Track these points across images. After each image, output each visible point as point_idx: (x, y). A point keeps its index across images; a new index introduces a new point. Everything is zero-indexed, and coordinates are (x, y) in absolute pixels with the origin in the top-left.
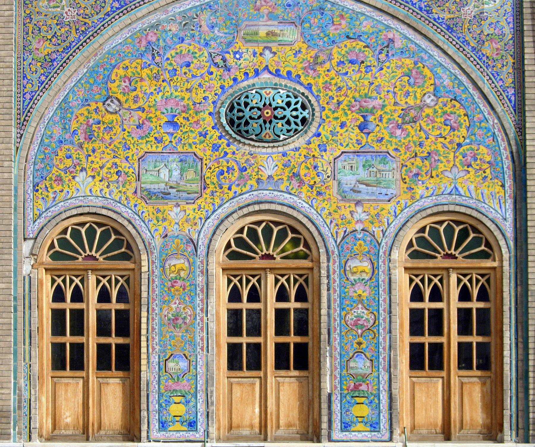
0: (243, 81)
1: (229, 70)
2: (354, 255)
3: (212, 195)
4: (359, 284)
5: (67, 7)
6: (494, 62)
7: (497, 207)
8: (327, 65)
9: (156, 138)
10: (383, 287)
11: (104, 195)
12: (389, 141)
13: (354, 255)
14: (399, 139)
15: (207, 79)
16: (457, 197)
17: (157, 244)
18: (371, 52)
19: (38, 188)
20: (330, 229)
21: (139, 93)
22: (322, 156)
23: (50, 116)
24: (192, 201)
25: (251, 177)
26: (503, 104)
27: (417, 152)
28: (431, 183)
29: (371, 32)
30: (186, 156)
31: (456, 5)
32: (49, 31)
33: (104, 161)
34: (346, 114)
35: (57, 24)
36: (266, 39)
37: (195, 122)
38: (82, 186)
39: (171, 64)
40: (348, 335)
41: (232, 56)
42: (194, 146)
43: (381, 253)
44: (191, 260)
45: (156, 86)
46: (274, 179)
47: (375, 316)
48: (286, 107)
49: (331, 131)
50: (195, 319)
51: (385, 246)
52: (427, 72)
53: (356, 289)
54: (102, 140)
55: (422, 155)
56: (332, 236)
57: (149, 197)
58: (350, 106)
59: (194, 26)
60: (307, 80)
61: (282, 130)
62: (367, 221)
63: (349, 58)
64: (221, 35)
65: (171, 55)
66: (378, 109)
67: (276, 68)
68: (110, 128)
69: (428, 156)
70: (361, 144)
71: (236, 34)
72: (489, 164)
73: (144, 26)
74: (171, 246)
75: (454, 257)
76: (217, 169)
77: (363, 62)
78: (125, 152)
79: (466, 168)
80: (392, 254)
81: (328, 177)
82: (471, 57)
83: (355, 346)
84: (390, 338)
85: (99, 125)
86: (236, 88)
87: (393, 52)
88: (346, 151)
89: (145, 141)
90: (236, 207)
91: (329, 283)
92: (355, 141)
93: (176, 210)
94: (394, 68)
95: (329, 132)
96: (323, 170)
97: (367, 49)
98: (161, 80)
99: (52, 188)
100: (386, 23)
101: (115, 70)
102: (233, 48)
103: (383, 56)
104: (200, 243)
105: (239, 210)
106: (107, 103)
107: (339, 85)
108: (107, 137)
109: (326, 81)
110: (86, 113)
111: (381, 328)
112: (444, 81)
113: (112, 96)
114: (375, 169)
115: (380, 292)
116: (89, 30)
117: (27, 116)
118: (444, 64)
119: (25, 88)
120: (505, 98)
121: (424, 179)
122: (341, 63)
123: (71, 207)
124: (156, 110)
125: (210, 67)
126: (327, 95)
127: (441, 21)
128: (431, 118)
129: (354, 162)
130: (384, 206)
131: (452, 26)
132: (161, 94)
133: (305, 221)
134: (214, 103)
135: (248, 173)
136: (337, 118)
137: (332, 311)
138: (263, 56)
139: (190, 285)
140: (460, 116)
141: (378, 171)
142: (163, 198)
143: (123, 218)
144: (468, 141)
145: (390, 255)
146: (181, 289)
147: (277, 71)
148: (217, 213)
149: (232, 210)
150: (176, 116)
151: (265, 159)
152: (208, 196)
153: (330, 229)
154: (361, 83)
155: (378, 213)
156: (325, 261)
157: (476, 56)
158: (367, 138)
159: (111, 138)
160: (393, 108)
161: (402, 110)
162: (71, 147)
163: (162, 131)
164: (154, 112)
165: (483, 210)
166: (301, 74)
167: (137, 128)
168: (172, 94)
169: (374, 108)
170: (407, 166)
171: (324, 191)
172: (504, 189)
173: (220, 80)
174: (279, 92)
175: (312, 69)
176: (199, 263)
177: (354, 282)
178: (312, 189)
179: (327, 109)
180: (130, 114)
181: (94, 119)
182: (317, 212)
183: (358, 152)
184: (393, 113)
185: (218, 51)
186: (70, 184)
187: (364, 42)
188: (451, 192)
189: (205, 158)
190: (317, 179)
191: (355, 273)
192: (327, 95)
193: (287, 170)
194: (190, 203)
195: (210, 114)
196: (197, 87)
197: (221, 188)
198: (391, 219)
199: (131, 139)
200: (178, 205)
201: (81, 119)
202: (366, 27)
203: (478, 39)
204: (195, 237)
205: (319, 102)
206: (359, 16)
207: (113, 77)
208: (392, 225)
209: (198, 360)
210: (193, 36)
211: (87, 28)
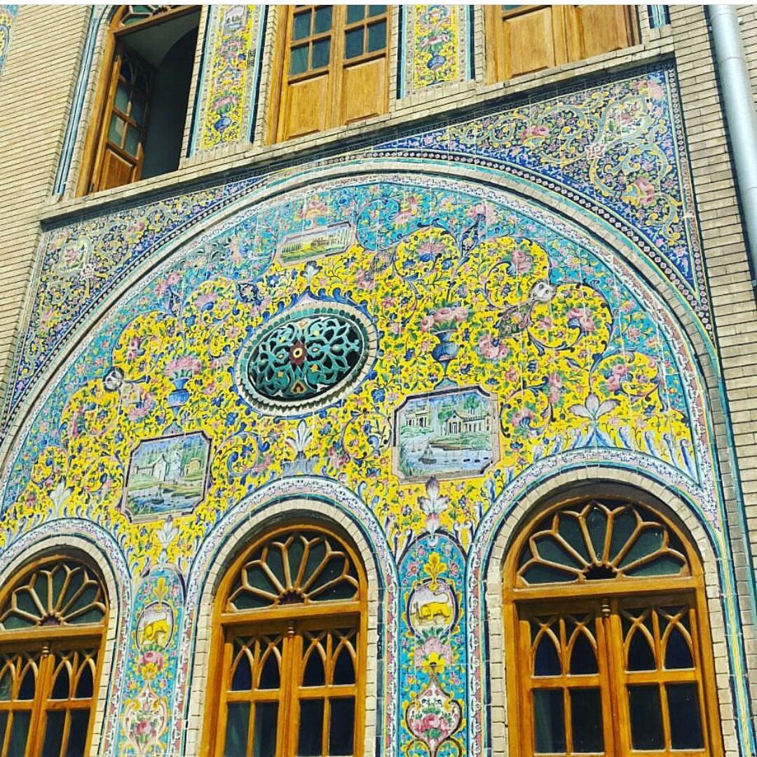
0: (276, 314)
2: (424, 582)
3: (219, 496)
4: (431, 641)
6: (646, 212)
7: (680, 464)
8: (389, 270)
10: (474, 645)
12: (480, 368)
13: (424, 582)
14: (495, 363)
16: (601, 451)
17: (134, 588)
20: (385, 536)
24: (190, 510)
25: (274, 459)
26: (668, 276)
27: (526, 379)
28: (551, 431)
29: (452, 211)
31: (576, 144)
34: (415, 337)
35: (71, 287)
37: (209, 384)
42: (203, 421)
43: (469, 575)
44: (176, 614)
45: (168, 343)
46: (305, 458)
47: (460, 708)
48: (326, 341)
51: (476, 560)
52: (536, 250)
53: (427, 651)
55: (534, 383)
57: (135, 510)
60: (361, 296)
61: (319, 376)
63: (421, 254)
64: (255, 258)
69: (545, 384)
70: (437, 380)
71: (273, 254)
72: (655, 383)
75: (605, 573)
77: (440, 255)
79: (612, 396)
80: (489, 574)
81: (386, 442)
82: (606, 212)
87: (485, 231)
88: (413, 395)
89: (143, 424)
90: (249, 512)
91: (380, 641)
92: (426, 377)
94: (485, 255)
95: (389, 369)
96: (378, 433)
97: (446, 236)
98: (176, 333)
100: (473, 194)
103: (468, 242)
104: (192, 582)
105: (252, 516)
107: (405, 295)
108: (99, 427)
109: (387, 293)
111: (471, 736)
114: (458, 420)
115: (470, 655)
118: (562, 232)
120: (672, 265)
127: (554, 171)
129: (424, 412)
132: (173, 353)
137: (384, 702)
138: (305, 275)
139: (169, 659)
141: (462, 420)
143: (97, 550)
144: (612, 348)
145: (485, 577)
146: (156, 668)
149: (242, 517)
150: (187, 380)
153: (385, 536)
155: (463, 496)
156: (375, 596)
157: (614, 210)
158: (445, 370)
160: (487, 314)
161: (500, 315)
163: (166, 406)
165: (653, 471)
167: (137, 407)
168: (185, 350)
169: (456, 319)
171: (377, 467)
173: (247, 319)
174: (320, 320)
175: (367, 280)
176: (186, 617)
177: (422, 638)
178: (360, 466)
179: (386, 334)
182: (367, 506)
183: (432, 394)
186: (43, 505)
188: (588, 443)
189: (215, 438)
190: (369, 449)
191: (426, 617)
194: (187, 513)
196: (217, 334)
200: (171, 519)
201: (75, 405)
202: (446, 205)
203: (614, 184)
206: (436, 193)
207: (121, 341)
208: (487, 518)
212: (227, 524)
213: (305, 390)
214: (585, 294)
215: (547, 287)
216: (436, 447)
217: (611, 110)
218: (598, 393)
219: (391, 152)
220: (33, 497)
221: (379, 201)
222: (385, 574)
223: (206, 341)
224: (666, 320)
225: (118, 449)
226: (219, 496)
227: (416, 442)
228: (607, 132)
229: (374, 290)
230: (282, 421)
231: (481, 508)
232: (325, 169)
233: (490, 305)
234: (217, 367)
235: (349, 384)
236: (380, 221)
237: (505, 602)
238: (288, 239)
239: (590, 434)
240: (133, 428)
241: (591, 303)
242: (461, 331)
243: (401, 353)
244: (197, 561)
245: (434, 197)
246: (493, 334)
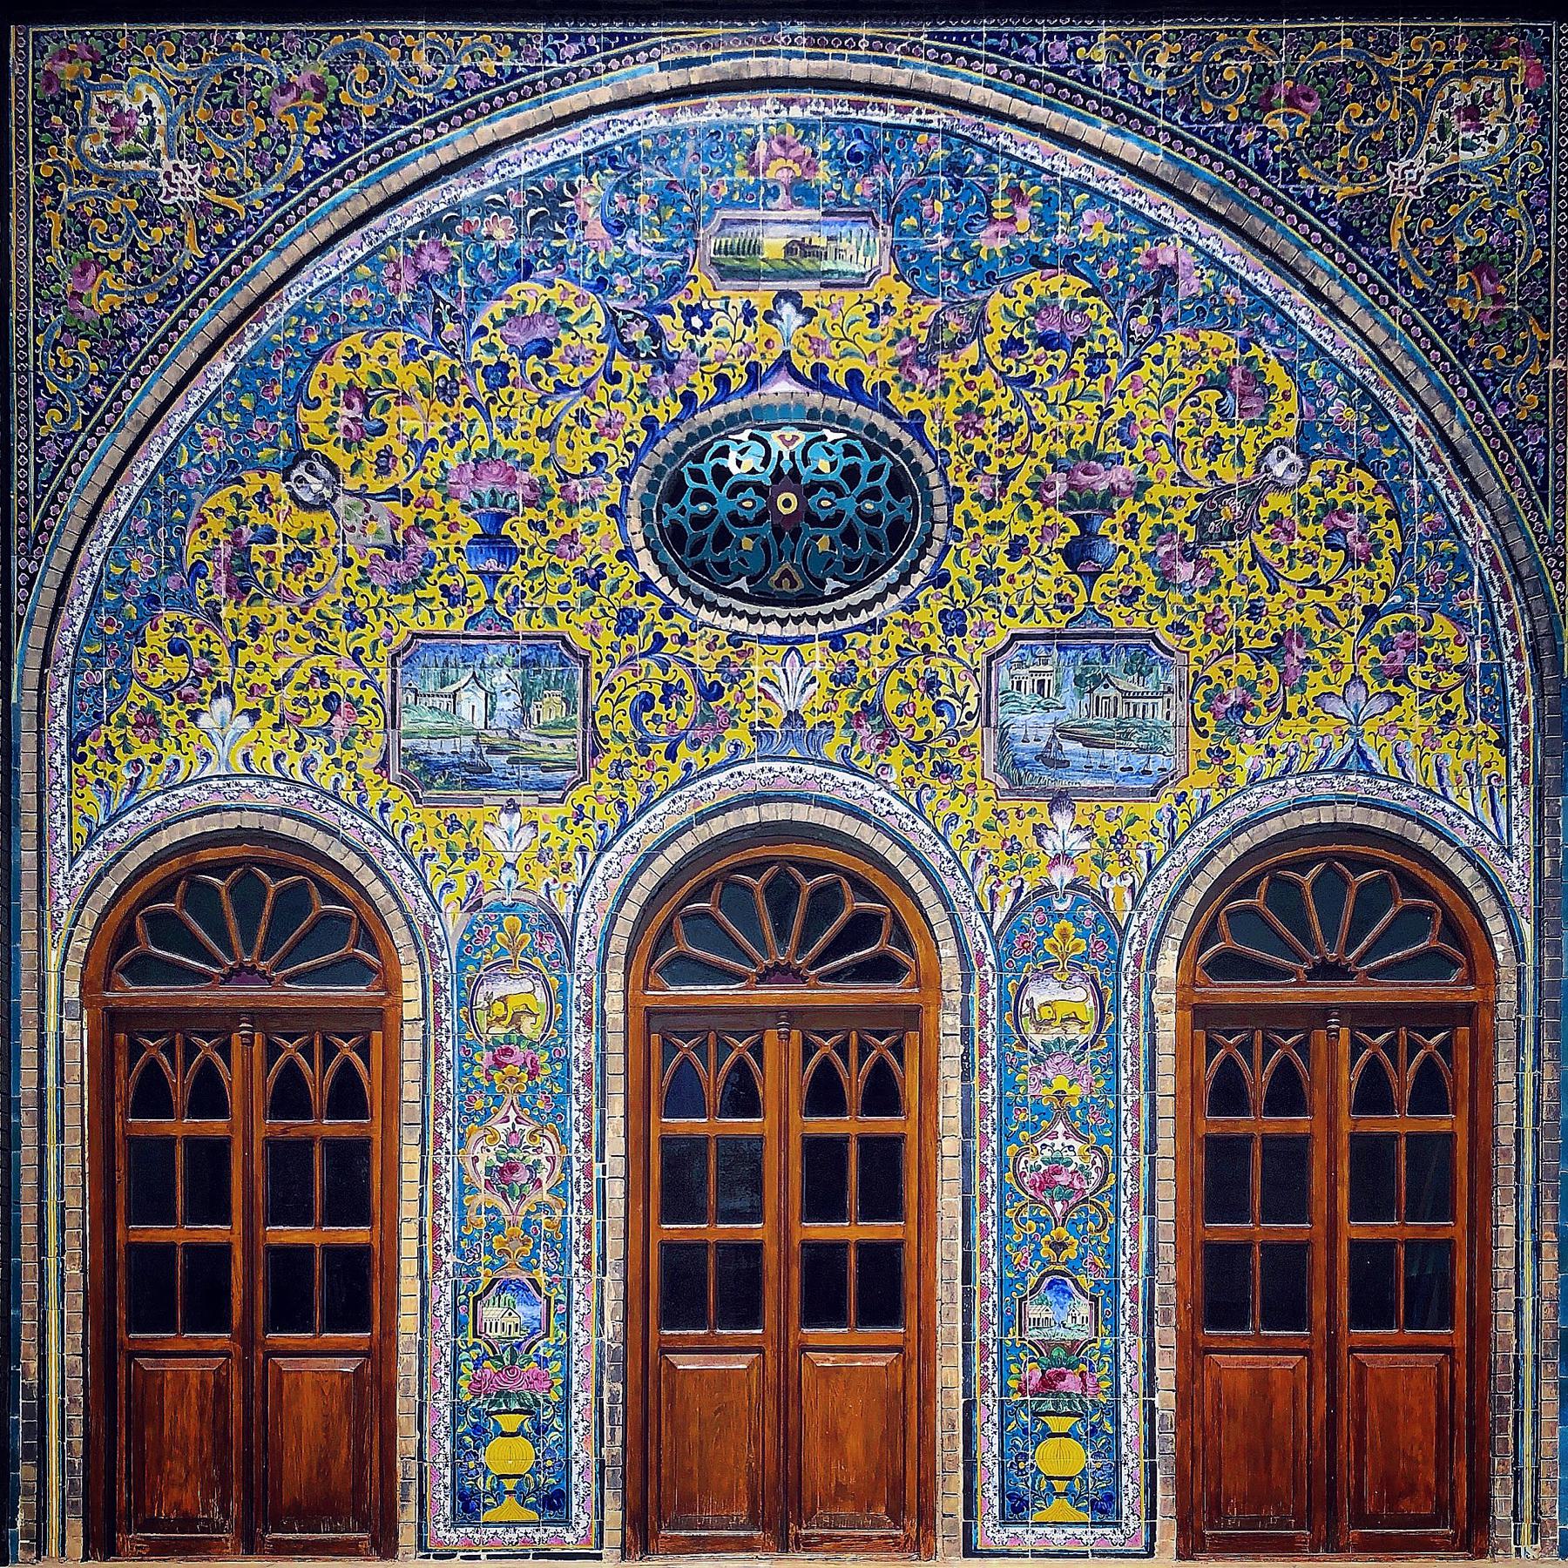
0: (712, 403)
1: (671, 369)
2: (1045, 966)
5: (171, 157)
8: (971, 353)
9: (445, 590)
10: (1129, 1068)
11: (286, 772)
14: (1187, 594)
15: (601, 397)
16: (1361, 778)
18: (1106, 309)
19: (85, 749)
20: (971, 884)
21: (394, 443)
22: (952, 649)
23: (122, 515)
26: (1509, 479)
27: (1243, 634)
30: (539, 648)
32: (116, 237)
34: (1027, 512)
35: (139, 214)
36: (783, 265)
38: (219, 743)
39: (491, 348)
40: (1024, 1220)
41: (680, 321)
42: (561, 616)
44: (555, 983)
45: (445, 418)
46: (804, 725)
47: (1106, 1159)
49: (979, 568)
51: (1137, 939)
52: (1276, 374)
53: (1049, 1073)
55: (1257, 644)
56: (979, 904)
58: (1040, 487)
59: (562, 225)
61: (831, 561)
62: (1089, 856)
64: (646, 252)
65: (492, 318)
66: (1125, 494)
67: (813, 361)
68: (304, 555)
70: (1072, 609)
72: (1463, 673)
73: (410, 223)
74: (493, 937)
76: (633, 692)
77: (1081, 343)
78: (352, 634)
79: (1390, 686)
82: (1416, 323)
83: (1046, 1252)
84: (1151, 1228)
85: (269, 547)
93: (508, 822)
94: (1175, 363)
97: (1092, 300)
98: (461, 399)
99: (127, 750)
100: (1152, 214)
101: (321, 367)
102: (680, 296)
104: (581, 930)
105: (699, 823)
106: (295, 473)
107: (1005, 417)
108: (296, 587)
109: (968, 404)
110: (230, 508)
112: (1329, 404)
113: (311, 451)
114: (1112, 692)
116: (238, 235)
117: (46, 514)
118: (1329, 348)
119: (43, 422)
120: (1518, 458)
121: (1261, 721)
122: (1012, 346)
123: (185, 810)
124: (445, 498)
125: (611, 357)
126: (969, 449)
128: (1285, 524)
129: (1048, 668)
130: (1139, 809)
131: (1356, 223)
132: (461, 445)
133: (895, 856)
134: (624, 474)
135: (728, 704)
136: (1002, 526)
139: (551, 1061)
140: (1374, 518)
141: (1120, 696)
142: (468, 784)
145: (1153, 965)
147: (819, 370)
149: (675, 821)
150: (506, 517)
151: (778, 658)
152: (604, 778)
154: (1073, 411)
155: (1119, 832)
157: (1430, 321)
159: (308, 589)
161: (1199, 498)
164: (439, 503)
165: (1441, 821)
166: (890, 382)
167: (388, 556)
168: (493, 444)
169: (1113, 491)
170: (1209, 681)
172: (1507, 754)
173: (642, 399)
175: (923, 366)
176: (576, 992)
178: (919, 756)
179: (967, 494)
180: (367, 510)
181: (255, 528)
182: (935, 830)
183: (1061, 636)
184: (1170, 509)
185: (636, 303)
186: (182, 738)
187: (1083, 277)
188: (1343, 762)
190: (937, 724)
191: (1049, 1022)
192: (969, 449)
193: (843, 696)
194: (551, 801)
195: (612, 511)
196: (572, 423)
197: (645, 752)
198: (1160, 849)
199: (367, 590)
200: (512, 808)
201: (216, 526)
202: (1095, 229)
204: (565, 908)
205: (943, 475)
207: (314, 390)
208: (1161, 871)
209: (575, 1296)
211: (231, 229)
213: (801, 585)
214: (1361, 486)
215: (1293, 457)
216: (1069, 738)
217: (1446, 91)
218: (1368, 678)
219: (971, 58)
220: (149, 722)
221: (943, 179)
222: (971, 947)
223: (548, 433)
224: (1495, 565)
225: (357, 643)
226: (619, 775)
228: (1433, 140)
229: (938, 392)
230: (746, 645)
231: (1149, 855)
232: (810, 56)
233: (1182, 474)
234: (580, 499)
235: (893, 588)
236: (947, 230)
237: (1180, 1005)
239: (1347, 748)
240: (386, 604)
241: (1368, 506)
243: (1000, 542)
244: (588, 894)
246: (1184, 534)
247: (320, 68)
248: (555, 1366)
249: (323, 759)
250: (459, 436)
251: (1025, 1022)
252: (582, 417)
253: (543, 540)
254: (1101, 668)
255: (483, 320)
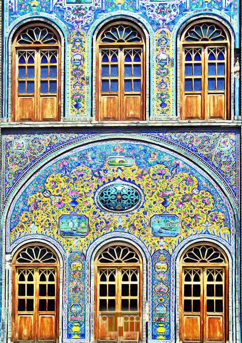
1: (101, 178)
8: (148, 176)
33: (43, 219)
50: (85, 288)
54: (42, 209)
58: (158, 194)
76: (95, 223)
77: (164, 174)
83: (159, 301)
86: (104, 186)
99: (19, 230)
110: (35, 197)
122: (154, 175)
132: (69, 189)
136: (151, 200)
145: (176, 261)
147: (124, 178)
148: (96, 241)
149: (102, 240)
162: (28, 212)
169: (169, 195)
195: (93, 198)
200: (77, 238)
202: (167, 159)
204: (85, 252)
207: (47, 181)
210: (84, 163)
212: (98, 242)
223: (82, 187)
227: (157, 227)
238: (110, 158)
242: (171, 198)
245: (162, 154)
247: (48, 137)
248: (83, 316)
249: (48, 232)
250: (69, 187)
251: (156, 268)
252: (88, 185)
253: (82, 202)
254: (168, 220)
255: (73, 171)
